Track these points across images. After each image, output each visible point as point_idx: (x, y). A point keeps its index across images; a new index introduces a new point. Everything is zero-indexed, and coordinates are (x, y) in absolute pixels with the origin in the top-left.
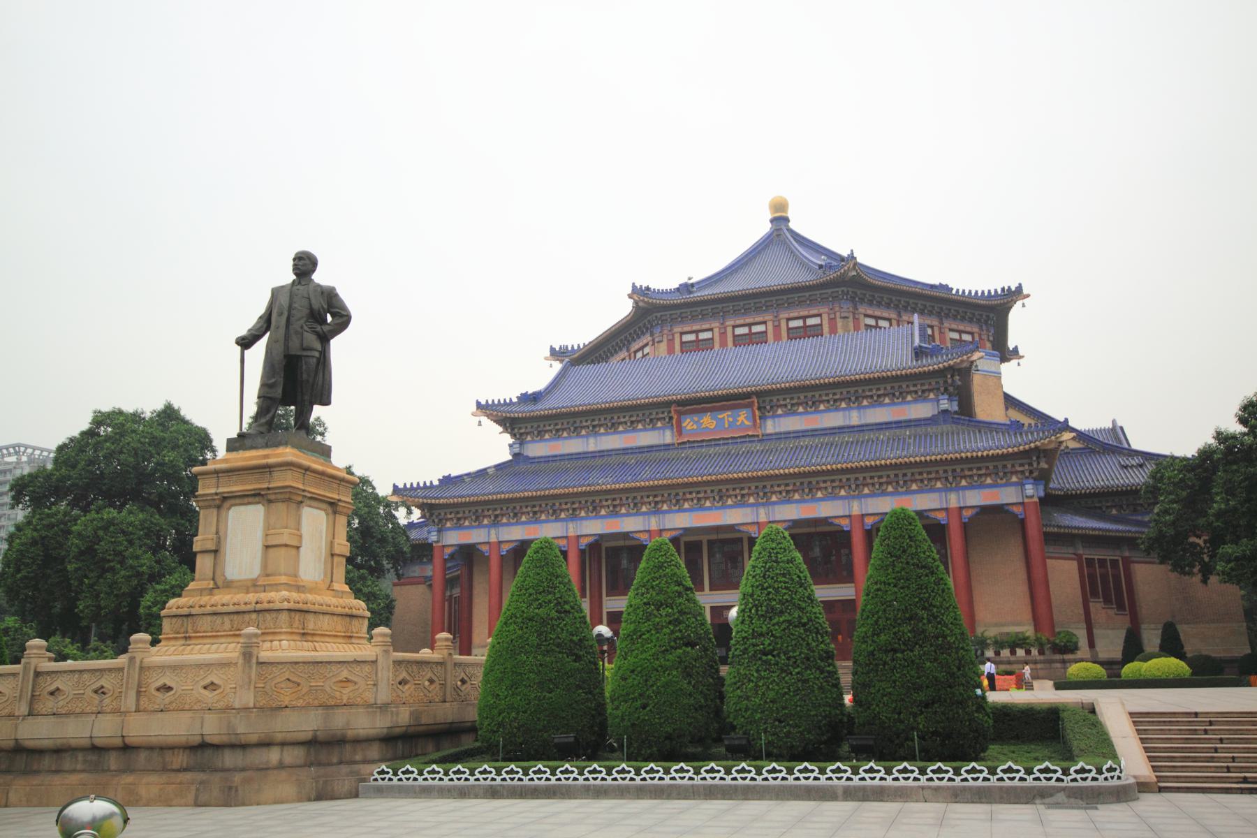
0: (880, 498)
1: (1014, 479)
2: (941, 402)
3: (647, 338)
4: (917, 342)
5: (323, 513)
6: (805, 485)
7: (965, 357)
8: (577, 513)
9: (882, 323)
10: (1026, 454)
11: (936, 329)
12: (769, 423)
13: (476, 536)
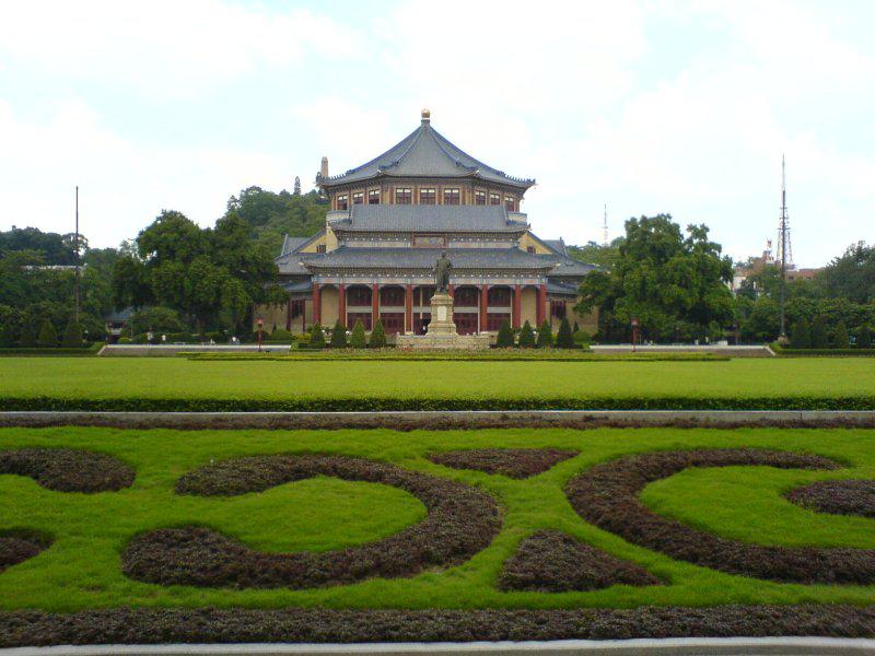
13: (335, 281)
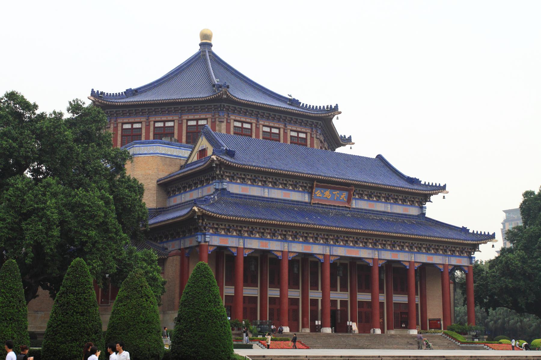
0: (422, 255)
12: (354, 202)
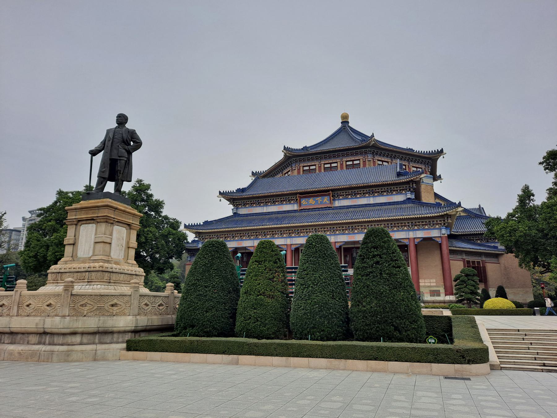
1: (437, 227)
2: (407, 195)
3: (289, 169)
4: (398, 170)
5: (124, 229)
6: (350, 228)
7: (418, 176)
8: (258, 236)
9: (385, 163)
10: (442, 216)
11: (407, 166)
